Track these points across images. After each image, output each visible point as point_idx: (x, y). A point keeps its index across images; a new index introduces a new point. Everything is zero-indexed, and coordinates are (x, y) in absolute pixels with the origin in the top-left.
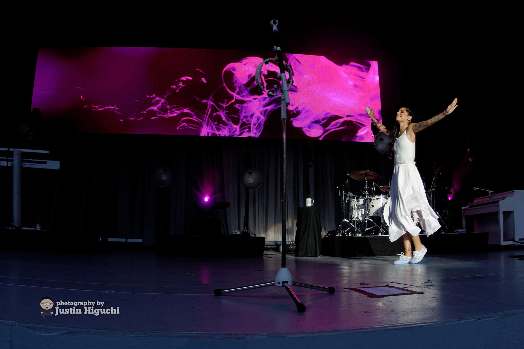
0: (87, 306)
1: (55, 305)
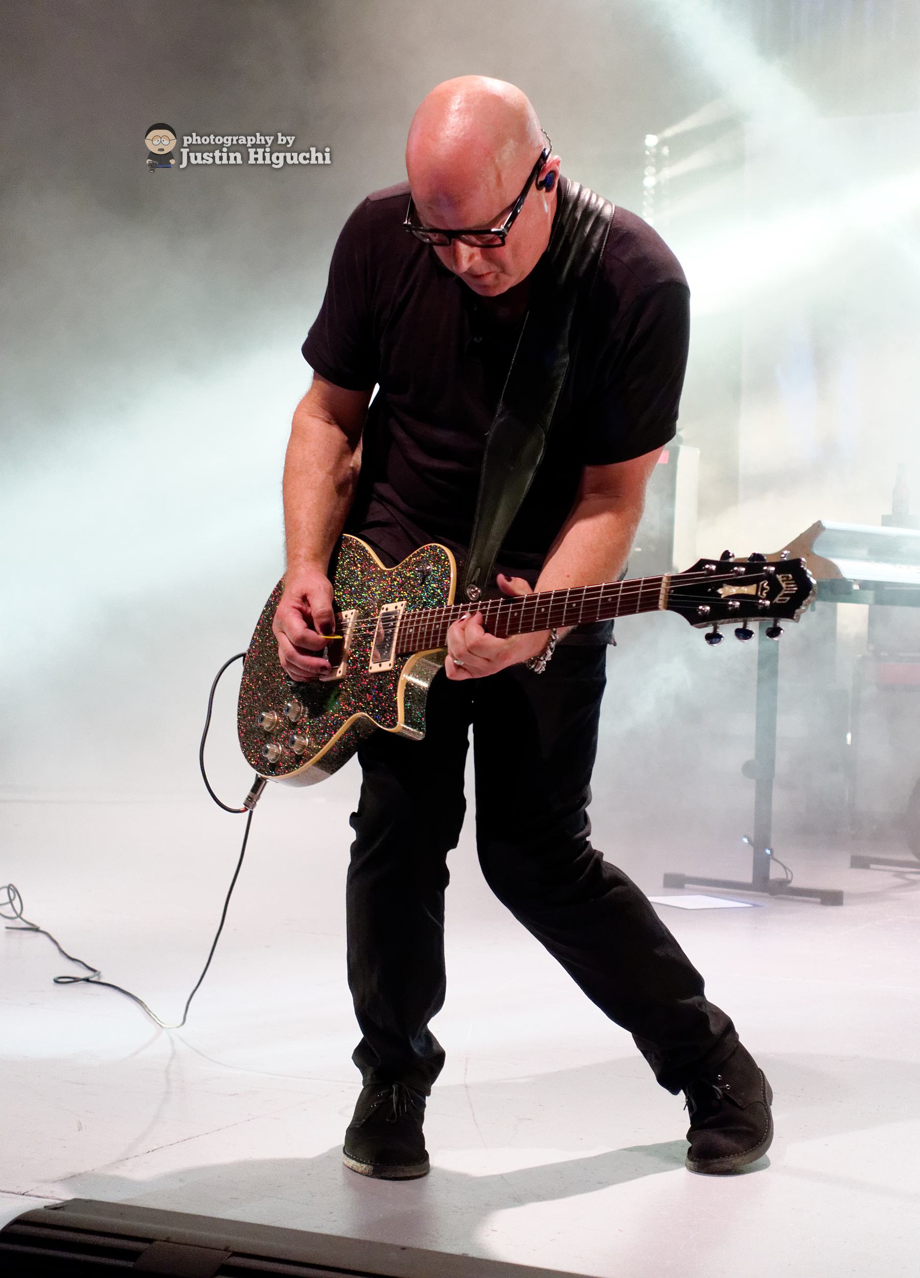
0: (253, 146)
1: (180, 144)
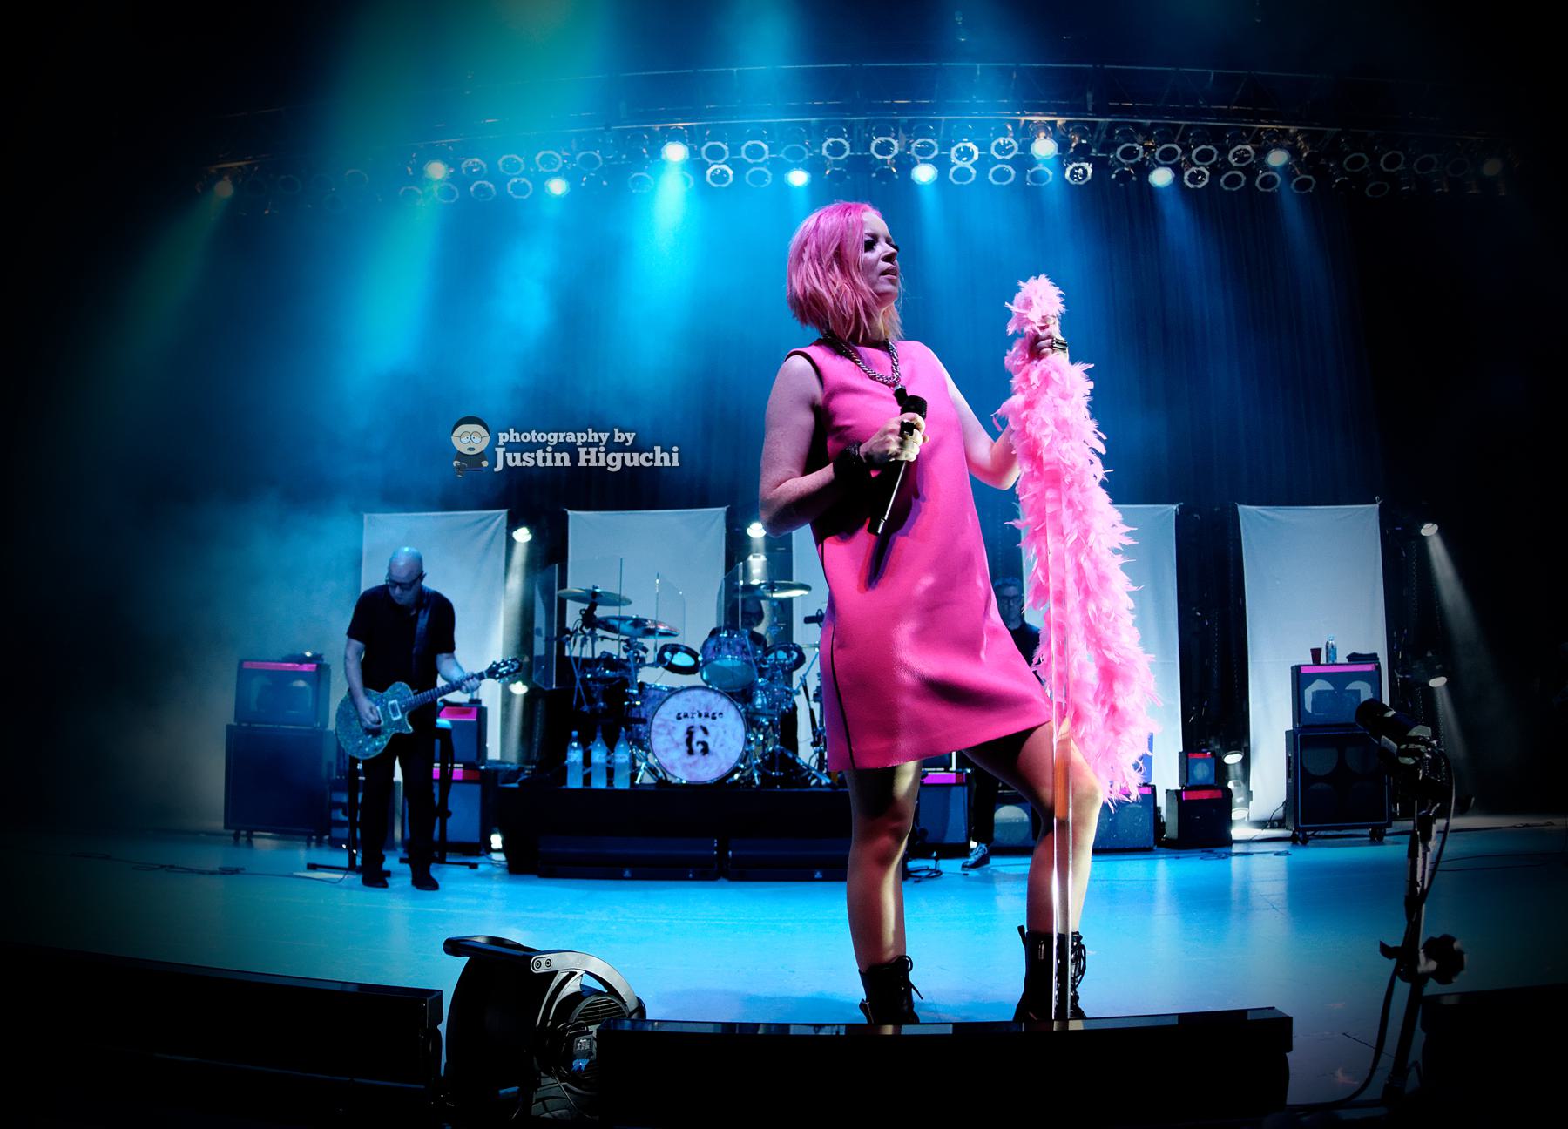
0: (587, 444)
1: (495, 442)
